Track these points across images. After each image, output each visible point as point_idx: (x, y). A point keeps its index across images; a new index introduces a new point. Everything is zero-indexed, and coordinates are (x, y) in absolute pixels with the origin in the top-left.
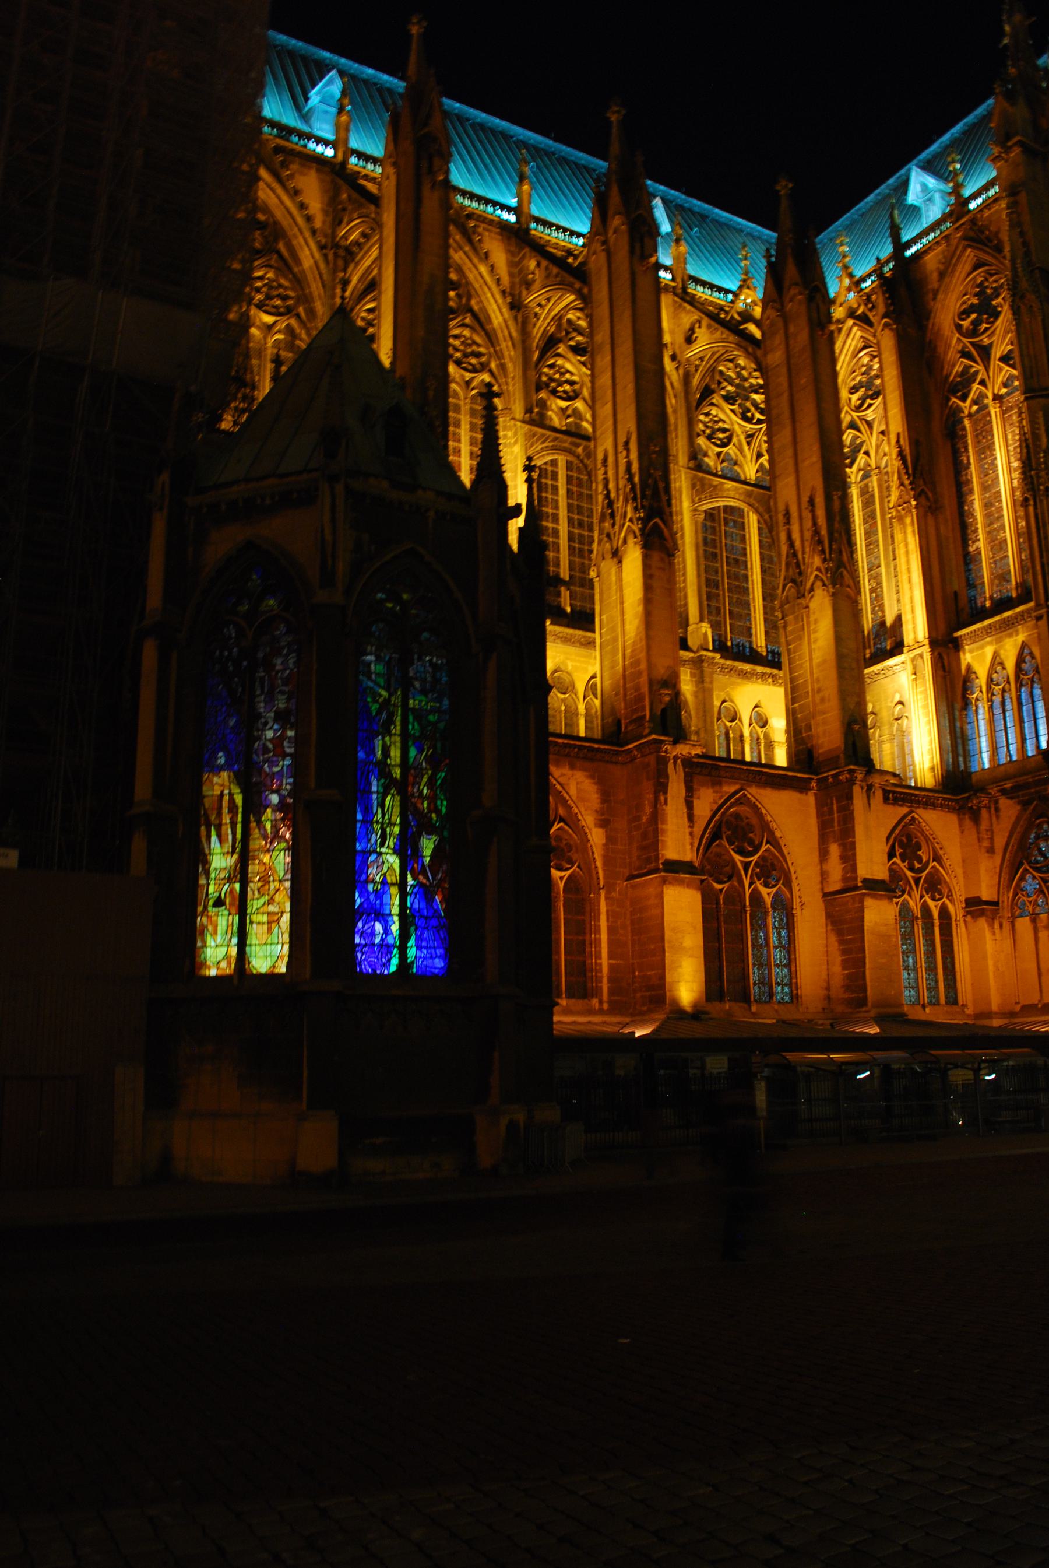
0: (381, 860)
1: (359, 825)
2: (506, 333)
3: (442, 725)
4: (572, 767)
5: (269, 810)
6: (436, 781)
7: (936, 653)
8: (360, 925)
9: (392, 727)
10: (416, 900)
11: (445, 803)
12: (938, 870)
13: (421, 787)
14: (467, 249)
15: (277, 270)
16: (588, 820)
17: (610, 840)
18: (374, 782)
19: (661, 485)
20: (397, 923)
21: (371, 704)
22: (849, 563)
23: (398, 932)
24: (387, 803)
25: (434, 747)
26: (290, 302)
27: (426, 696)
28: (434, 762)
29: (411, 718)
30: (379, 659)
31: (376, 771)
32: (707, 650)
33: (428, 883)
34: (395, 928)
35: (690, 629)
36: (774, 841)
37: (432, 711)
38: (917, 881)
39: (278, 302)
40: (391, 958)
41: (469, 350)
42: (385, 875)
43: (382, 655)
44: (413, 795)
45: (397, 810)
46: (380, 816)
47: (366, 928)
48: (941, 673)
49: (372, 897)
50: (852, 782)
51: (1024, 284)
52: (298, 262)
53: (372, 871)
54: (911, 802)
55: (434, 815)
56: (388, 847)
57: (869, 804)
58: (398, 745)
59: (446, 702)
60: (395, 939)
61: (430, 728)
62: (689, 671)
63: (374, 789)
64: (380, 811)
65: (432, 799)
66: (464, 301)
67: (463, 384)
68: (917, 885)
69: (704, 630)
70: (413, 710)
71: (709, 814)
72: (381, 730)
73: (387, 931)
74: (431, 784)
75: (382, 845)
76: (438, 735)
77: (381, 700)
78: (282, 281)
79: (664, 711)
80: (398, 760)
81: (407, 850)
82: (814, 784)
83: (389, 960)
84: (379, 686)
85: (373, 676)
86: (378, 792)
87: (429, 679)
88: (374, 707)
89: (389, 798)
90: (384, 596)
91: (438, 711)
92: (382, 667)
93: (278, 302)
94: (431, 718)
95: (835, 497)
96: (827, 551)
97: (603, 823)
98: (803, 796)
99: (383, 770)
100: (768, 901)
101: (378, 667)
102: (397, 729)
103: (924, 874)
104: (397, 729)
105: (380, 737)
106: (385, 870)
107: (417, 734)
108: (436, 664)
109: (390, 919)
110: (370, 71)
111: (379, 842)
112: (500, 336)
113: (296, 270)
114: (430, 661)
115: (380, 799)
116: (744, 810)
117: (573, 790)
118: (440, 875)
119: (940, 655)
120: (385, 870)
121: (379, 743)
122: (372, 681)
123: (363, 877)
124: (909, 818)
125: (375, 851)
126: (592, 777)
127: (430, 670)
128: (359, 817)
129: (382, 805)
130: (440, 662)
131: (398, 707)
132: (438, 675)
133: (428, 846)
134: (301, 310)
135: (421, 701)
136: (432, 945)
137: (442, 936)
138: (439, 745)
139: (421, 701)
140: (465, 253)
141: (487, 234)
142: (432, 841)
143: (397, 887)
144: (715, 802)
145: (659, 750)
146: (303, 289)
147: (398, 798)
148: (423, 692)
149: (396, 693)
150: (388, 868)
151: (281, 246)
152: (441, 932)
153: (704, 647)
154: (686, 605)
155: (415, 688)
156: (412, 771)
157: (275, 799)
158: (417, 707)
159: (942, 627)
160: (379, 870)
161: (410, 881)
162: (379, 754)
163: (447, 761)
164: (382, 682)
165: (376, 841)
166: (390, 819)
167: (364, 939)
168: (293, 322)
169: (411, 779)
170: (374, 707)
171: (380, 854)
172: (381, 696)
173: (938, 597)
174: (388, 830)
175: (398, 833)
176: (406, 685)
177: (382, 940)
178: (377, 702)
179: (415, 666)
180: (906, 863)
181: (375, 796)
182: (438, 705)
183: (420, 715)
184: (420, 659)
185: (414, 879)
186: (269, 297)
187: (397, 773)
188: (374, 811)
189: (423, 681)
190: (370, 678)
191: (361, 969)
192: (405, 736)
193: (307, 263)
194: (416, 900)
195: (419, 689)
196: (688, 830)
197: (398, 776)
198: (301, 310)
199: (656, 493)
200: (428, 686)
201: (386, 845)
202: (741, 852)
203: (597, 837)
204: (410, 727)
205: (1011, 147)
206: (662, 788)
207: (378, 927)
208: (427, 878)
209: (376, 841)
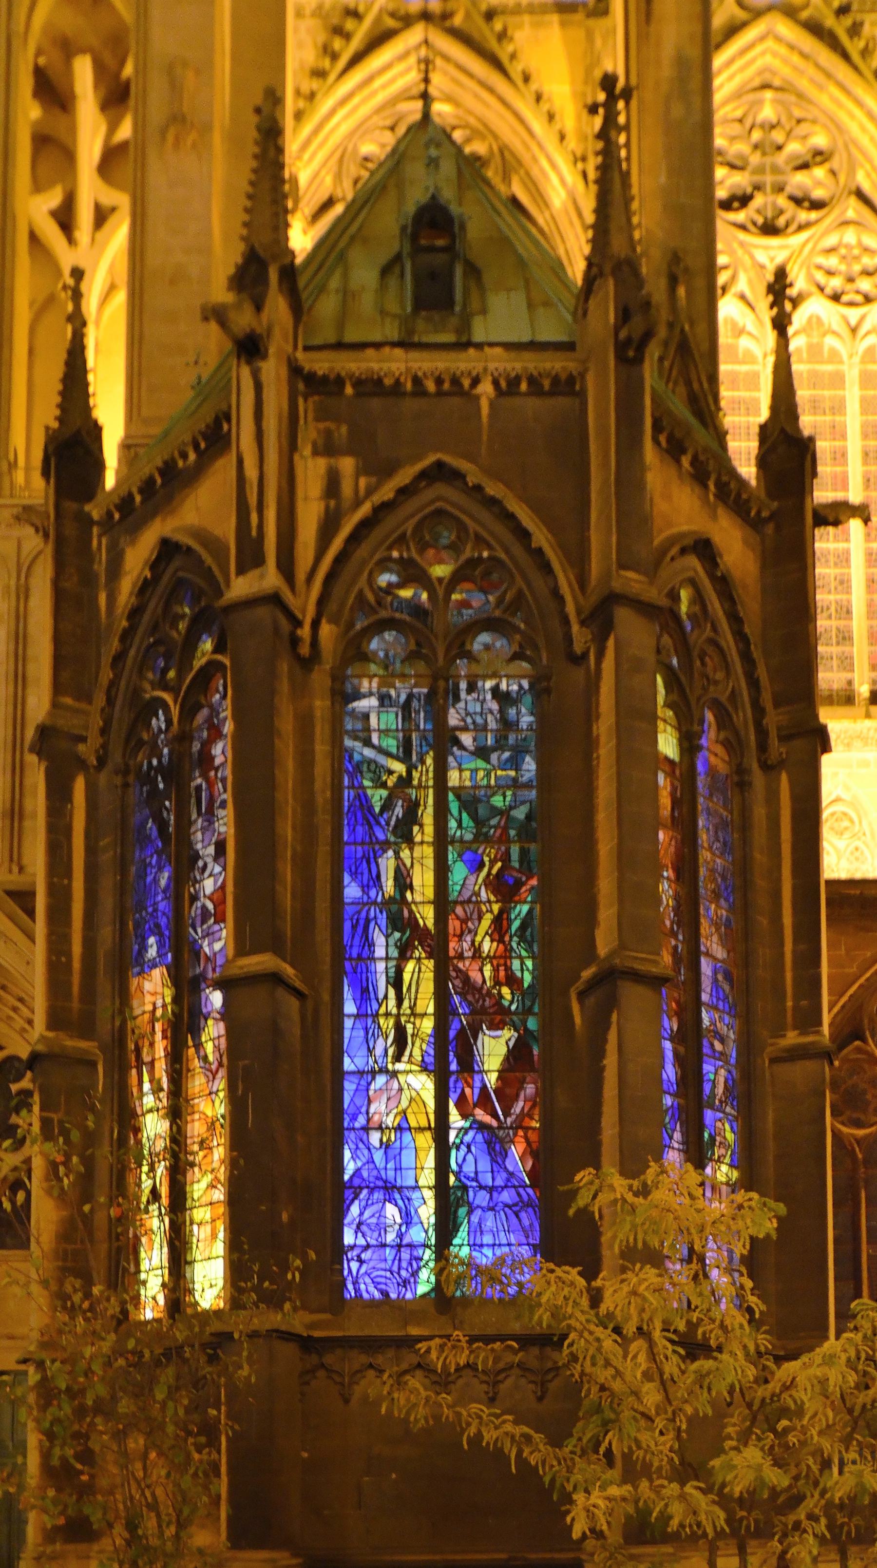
0: (396, 1086)
1: (348, 1023)
3: (520, 813)
5: (210, 1022)
6: (510, 922)
8: (355, 1210)
9: (416, 829)
10: (470, 1157)
11: (529, 963)
13: (478, 939)
18: (379, 940)
20: (431, 1203)
21: (369, 792)
23: (433, 1220)
24: (407, 977)
25: (506, 858)
27: (488, 761)
29: (454, 806)
31: (383, 919)
33: (494, 1123)
34: (427, 1212)
37: (500, 788)
40: (419, 1268)
42: (404, 1112)
43: (393, 692)
44: (461, 957)
45: (428, 987)
46: (392, 1002)
47: (367, 1214)
49: (378, 1156)
53: (378, 1107)
55: (506, 991)
56: (410, 1061)
58: (430, 863)
59: (530, 765)
60: (426, 1232)
61: (494, 822)
63: (380, 952)
64: (392, 993)
65: (503, 959)
70: (458, 792)
72: (392, 839)
73: (408, 1218)
75: (398, 1058)
76: (512, 833)
80: (430, 893)
83: (415, 1274)
84: (389, 754)
85: (375, 739)
86: (387, 958)
87: (492, 724)
88: (377, 797)
90: (394, 578)
91: (515, 784)
92: (392, 716)
94: (497, 801)
101: (383, 717)
102: (426, 831)
104: (426, 831)
105: (390, 853)
106: (404, 1103)
107: (469, 837)
108: (508, 693)
109: (415, 1195)
111: (391, 1052)
114: (495, 691)
115: (392, 971)
118: (521, 1104)
120: (404, 1103)
121: (387, 864)
122: (373, 747)
123: (361, 1121)
125: (384, 1070)
127: (495, 706)
128: (350, 1007)
129: (397, 982)
130: (515, 687)
131: (427, 787)
132: (512, 712)
135: (474, 771)
136: (504, 1241)
137: (526, 1222)
138: (515, 850)
139: (474, 771)
142: (503, 1041)
143: (428, 1135)
147: (430, 964)
148: (482, 752)
149: (423, 762)
150: (411, 1100)
152: (523, 1215)
155: (462, 747)
156: (459, 910)
158: (468, 783)
160: (393, 1103)
161: (455, 1119)
162: (389, 886)
163: (534, 882)
164: (391, 744)
165: (386, 1051)
166: (412, 1008)
167: (364, 1236)
169: (453, 925)
170: (377, 797)
171: (394, 1074)
172: (391, 772)
174: (409, 1027)
175: (429, 1031)
177: (400, 1235)
179: (461, 705)
181: (381, 966)
182: (512, 773)
185: (464, 1116)
187: (427, 916)
188: (381, 996)
190: (367, 743)
191: (357, 1290)
192: (441, 841)
194: (470, 1157)
195: (472, 748)
197: (430, 924)
201: (405, 1058)
204: (453, 824)
207: (391, 1211)
208: (495, 1115)
209: (386, 1051)
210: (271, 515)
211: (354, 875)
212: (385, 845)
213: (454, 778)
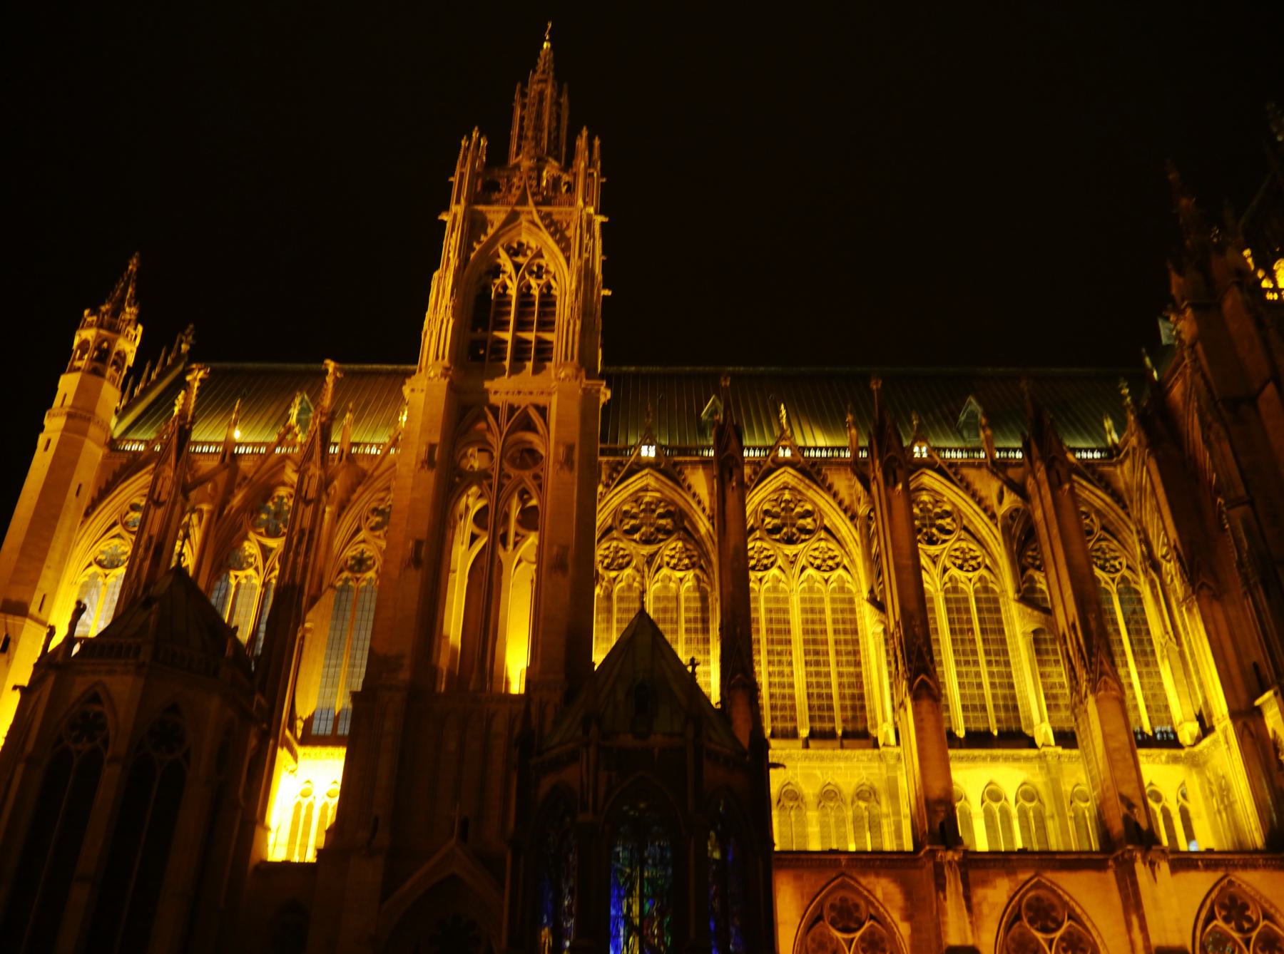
2: (851, 537)
3: (667, 887)
4: (877, 875)
7: (1240, 723)
12: (1272, 929)
14: (815, 487)
15: (684, 540)
16: (895, 916)
17: (915, 931)
19: (925, 649)
22: (1111, 670)
26: (695, 559)
28: (662, 913)
30: (624, 849)
32: (1049, 746)
35: (1035, 729)
36: (1073, 917)
38: (1247, 942)
39: (686, 561)
41: (826, 556)
45: (637, 946)
48: (1248, 740)
50: (1133, 860)
51: (1209, 418)
52: (697, 530)
54: (1226, 866)
57: (1155, 878)
59: (670, 871)
62: (1037, 766)
65: (661, 936)
66: (818, 523)
67: (823, 582)
68: (1248, 946)
69: (1043, 730)
70: (648, 879)
71: (1005, 900)
74: (659, 927)
77: (626, 875)
78: (689, 546)
79: (942, 824)
82: (1110, 863)
88: (622, 881)
89: (631, 939)
93: (686, 561)
95: (1091, 619)
96: (1088, 665)
97: (908, 917)
98: (1102, 875)
99: (628, 919)
103: (1254, 935)
110: (762, 369)
112: (848, 540)
113: (696, 537)
116: (1041, 893)
117: (879, 894)
119: (1245, 725)
124: (1226, 881)
126: (895, 881)
129: (627, 943)
134: (702, 562)
140: (814, 490)
144: (1011, 889)
145: (934, 857)
146: (702, 549)
147: (637, 939)
148: (655, 865)
151: (686, 523)
153: (1046, 743)
154: (1030, 710)
157: (568, 944)
159: (1243, 696)
162: (625, 910)
164: (627, 863)
168: (698, 572)
169: (645, 925)
170: (622, 881)
173: (1235, 671)
176: (643, 863)
178: (623, 876)
180: (1233, 924)
183: (651, 881)
184: (652, 844)
186: (680, 560)
187: (637, 921)
189: (654, 859)
192: (642, 897)
193: (703, 531)
196: (967, 920)
198: (702, 562)
199: (920, 656)
200: (657, 861)
202: (1045, 930)
203: (904, 929)
204: (645, 890)
205: (1185, 309)
206: (941, 887)
210: (591, 795)
211: (614, 907)
212: (623, 898)
213: (646, 874)
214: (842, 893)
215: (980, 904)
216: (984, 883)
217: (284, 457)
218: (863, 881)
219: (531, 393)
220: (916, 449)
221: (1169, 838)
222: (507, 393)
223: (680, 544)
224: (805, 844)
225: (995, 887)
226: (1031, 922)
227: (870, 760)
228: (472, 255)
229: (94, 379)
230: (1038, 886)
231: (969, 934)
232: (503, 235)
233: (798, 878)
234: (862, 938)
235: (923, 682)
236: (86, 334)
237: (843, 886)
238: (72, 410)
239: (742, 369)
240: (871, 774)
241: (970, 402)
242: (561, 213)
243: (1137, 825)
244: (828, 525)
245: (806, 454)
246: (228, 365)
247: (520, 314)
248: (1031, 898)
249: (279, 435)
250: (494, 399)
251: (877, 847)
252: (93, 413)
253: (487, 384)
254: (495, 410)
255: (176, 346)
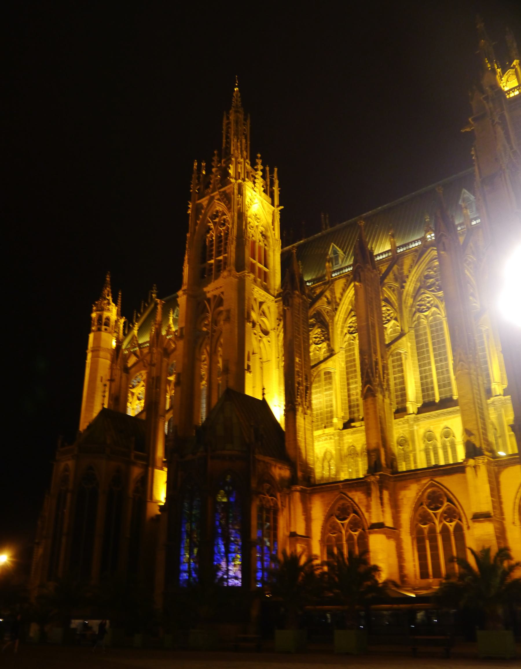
4: (356, 491)
36: (450, 500)
39: (323, 338)
57: (476, 475)
78: (324, 330)
79: (375, 462)
81: (191, 553)
100: (452, 529)
117: (356, 500)
126: (363, 493)
133: (195, 551)
141: (382, 267)
196: (381, 509)
214: (341, 502)
215: (402, 499)
216: (405, 488)
217: (170, 339)
218: (350, 494)
219: (221, 287)
220: (428, 236)
221: (435, 459)
222: (212, 291)
223: (320, 330)
224: (457, 461)
225: (410, 490)
226: (428, 506)
227: (404, 423)
228: (197, 227)
229: (98, 332)
230: (432, 485)
231: (381, 517)
232: (209, 211)
233: (323, 497)
234: (350, 523)
235: (369, 388)
236: (94, 315)
237: (342, 498)
238: (92, 349)
239: (370, 212)
240: (404, 431)
241: (465, 193)
242: (229, 189)
243: (474, 445)
244: (387, 297)
245: (312, 283)
246: (168, 298)
247: (219, 247)
248: (430, 493)
249: (166, 330)
250: (209, 295)
251: (409, 469)
252: (100, 347)
253: (205, 289)
254: (209, 300)
255: (150, 296)
